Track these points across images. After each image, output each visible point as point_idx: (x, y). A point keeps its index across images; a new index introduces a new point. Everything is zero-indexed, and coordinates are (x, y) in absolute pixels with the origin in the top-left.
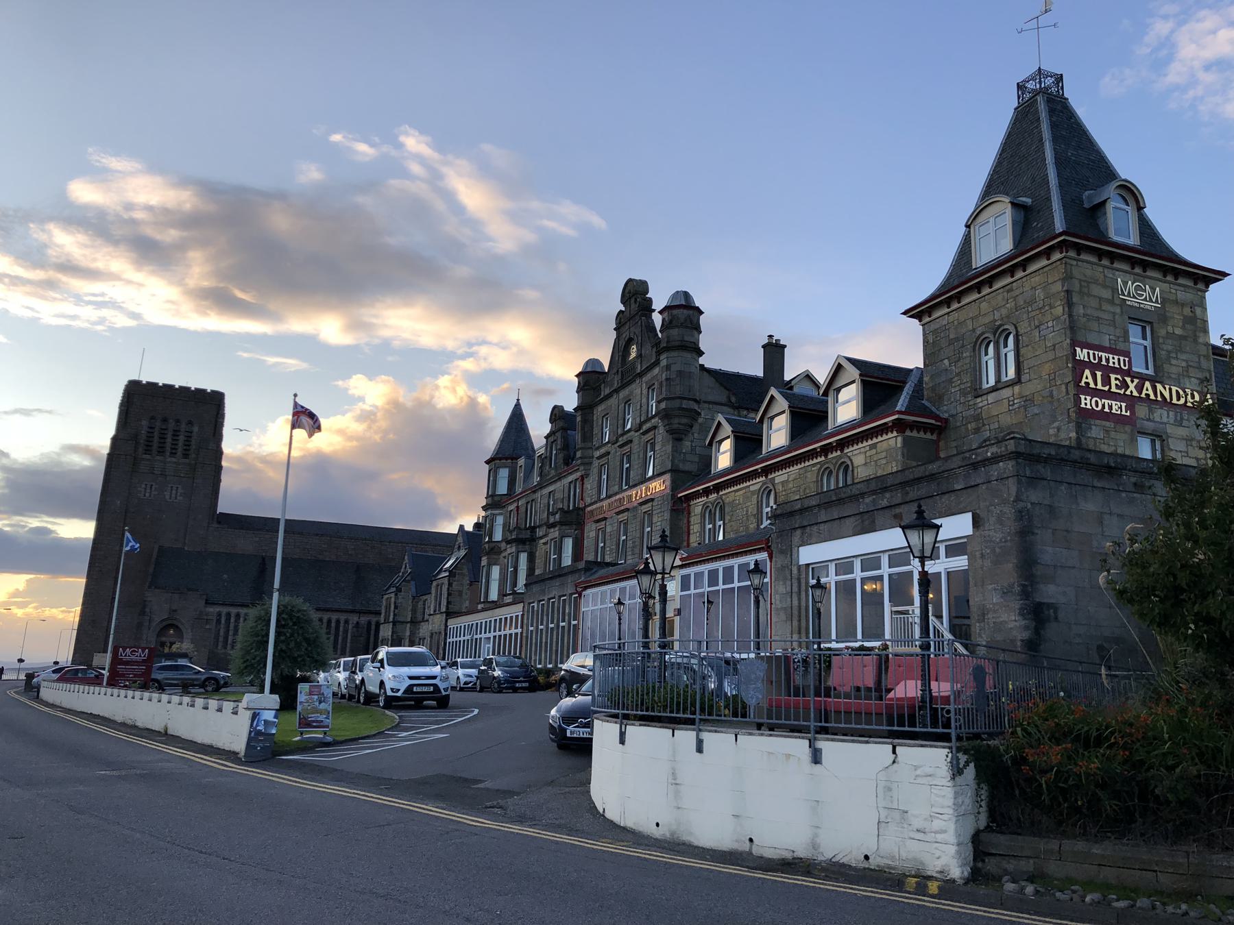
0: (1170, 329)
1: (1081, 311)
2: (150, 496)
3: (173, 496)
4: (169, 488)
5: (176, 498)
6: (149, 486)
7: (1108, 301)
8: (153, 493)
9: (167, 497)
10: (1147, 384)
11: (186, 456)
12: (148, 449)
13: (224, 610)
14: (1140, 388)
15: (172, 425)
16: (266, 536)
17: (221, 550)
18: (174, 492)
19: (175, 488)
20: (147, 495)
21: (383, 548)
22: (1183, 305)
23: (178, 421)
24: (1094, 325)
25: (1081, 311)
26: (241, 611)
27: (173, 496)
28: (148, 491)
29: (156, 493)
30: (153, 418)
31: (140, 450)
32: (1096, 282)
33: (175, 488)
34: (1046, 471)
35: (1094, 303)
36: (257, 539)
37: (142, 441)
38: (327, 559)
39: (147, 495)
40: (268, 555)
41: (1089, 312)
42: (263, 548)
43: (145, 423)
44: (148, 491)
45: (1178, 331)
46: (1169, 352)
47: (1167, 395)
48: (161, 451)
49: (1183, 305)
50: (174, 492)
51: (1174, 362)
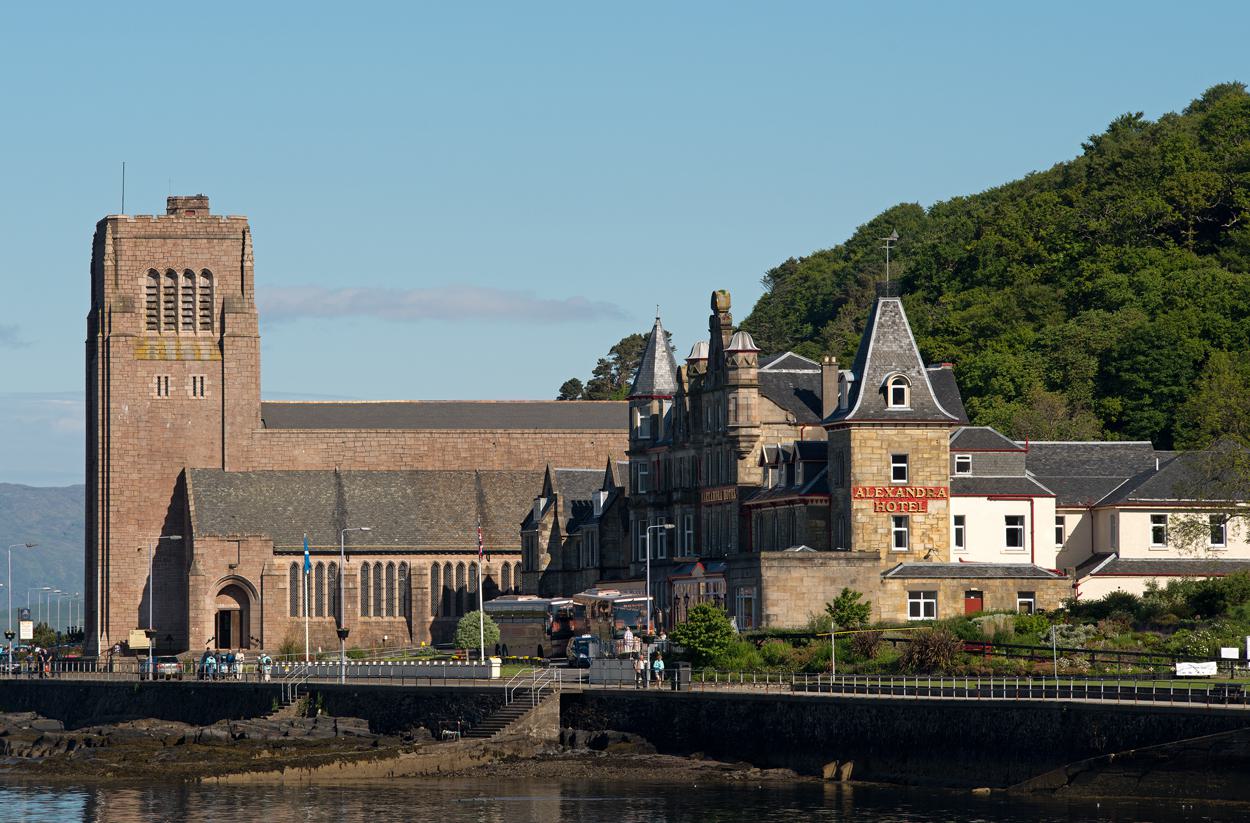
0: (920, 456)
1: (860, 457)
2: (167, 392)
3: (198, 390)
4: (192, 380)
5: (202, 395)
6: (163, 379)
7: (877, 448)
8: (169, 389)
9: (191, 393)
10: (901, 489)
11: (207, 326)
12: (153, 324)
14: (894, 492)
15: (182, 281)
16: (336, 440)
17: (275, 468)
18: (198, 385)
19: (198, 379)
20: (163, 392)
21: (514, 443)
22: (931, 440)
23: (189, 274)
24: (868, 463)
25: (860, 457)
26: (322, 560)
27: (198, 390)
28: (163, 387)
29: (174, 388)
30: (154, 274)
31: (143, 324)
32: (871, 439)
33: (198, 379)
34: (775, 563)
35: (869, 450)
36: (325, 446)
37: (142, 311)
38: (430, 469)
39: (163, 392)
40: (342, 468)
41: (864, 456)
42: (335, 458)
43: (145, 281)
44: (163, 387)
45: (926, 456)
46: (918, 468)
47: (913, 493)
48: (173, 323)
49: (931, 440)
50: (198, 385)
51: (920, 474)
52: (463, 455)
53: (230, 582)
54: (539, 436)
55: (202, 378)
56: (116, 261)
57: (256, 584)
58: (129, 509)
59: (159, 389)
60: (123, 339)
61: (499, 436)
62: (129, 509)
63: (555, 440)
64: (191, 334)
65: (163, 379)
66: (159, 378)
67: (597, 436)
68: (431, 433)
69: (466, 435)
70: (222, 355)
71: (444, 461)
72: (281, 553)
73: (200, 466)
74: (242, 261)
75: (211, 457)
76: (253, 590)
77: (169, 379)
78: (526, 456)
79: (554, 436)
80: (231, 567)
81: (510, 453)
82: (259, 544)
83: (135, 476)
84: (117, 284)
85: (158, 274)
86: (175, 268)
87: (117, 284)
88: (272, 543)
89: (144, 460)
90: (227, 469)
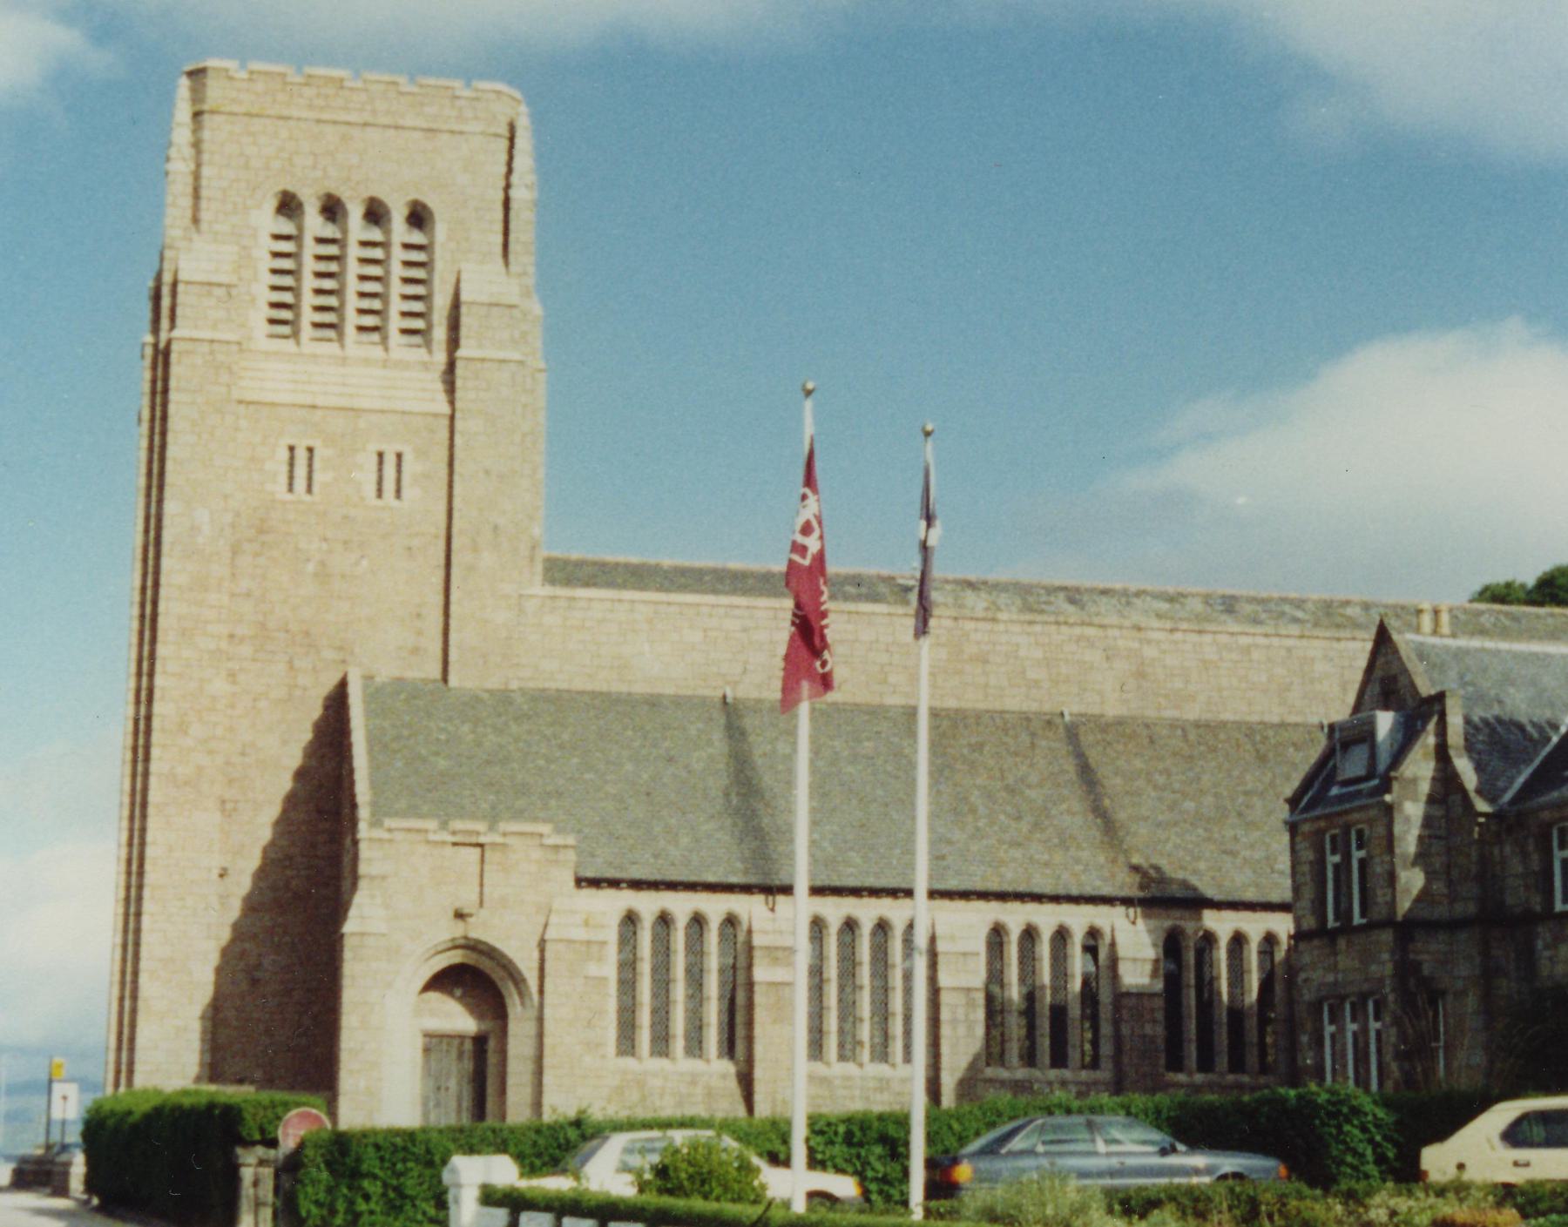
6: (301, 456)
9: (371, 488)
13: (648, 904)
52: (1032, 674)
53: (456, 957)
54: (1207, 638)
55: (399, 456)
56: (199, 165)
57: (527, 965)
58: (200, 768)
59: (291, 477)
60: (206, 348)
61: (1116, 632)
62: (200, 768)
63: (1247, 650)
64: (378, 352)
65: (301, 456)
66: (292, 449)
67: (1343, 645)
68: (956, 619)
69: (1038, 628)
70: (452, 402)
71: (986, 686)
72: (595, 883)
73: (385, 672)
74: (508, 187)
75: (415, 651)
76: (518, 980)
77: (317, 453)
78: (1178, 684)
79: (1244, 640)
80: (460, 915)
81: (1141, 675)
82: (537, 854)
83: (220, 686)
84: (196, 220)
85: (300, 206)
86: (344, 194)
87: (196, 220)
88: (571, 856)
89: (246, 650)
90: (454, 681)
